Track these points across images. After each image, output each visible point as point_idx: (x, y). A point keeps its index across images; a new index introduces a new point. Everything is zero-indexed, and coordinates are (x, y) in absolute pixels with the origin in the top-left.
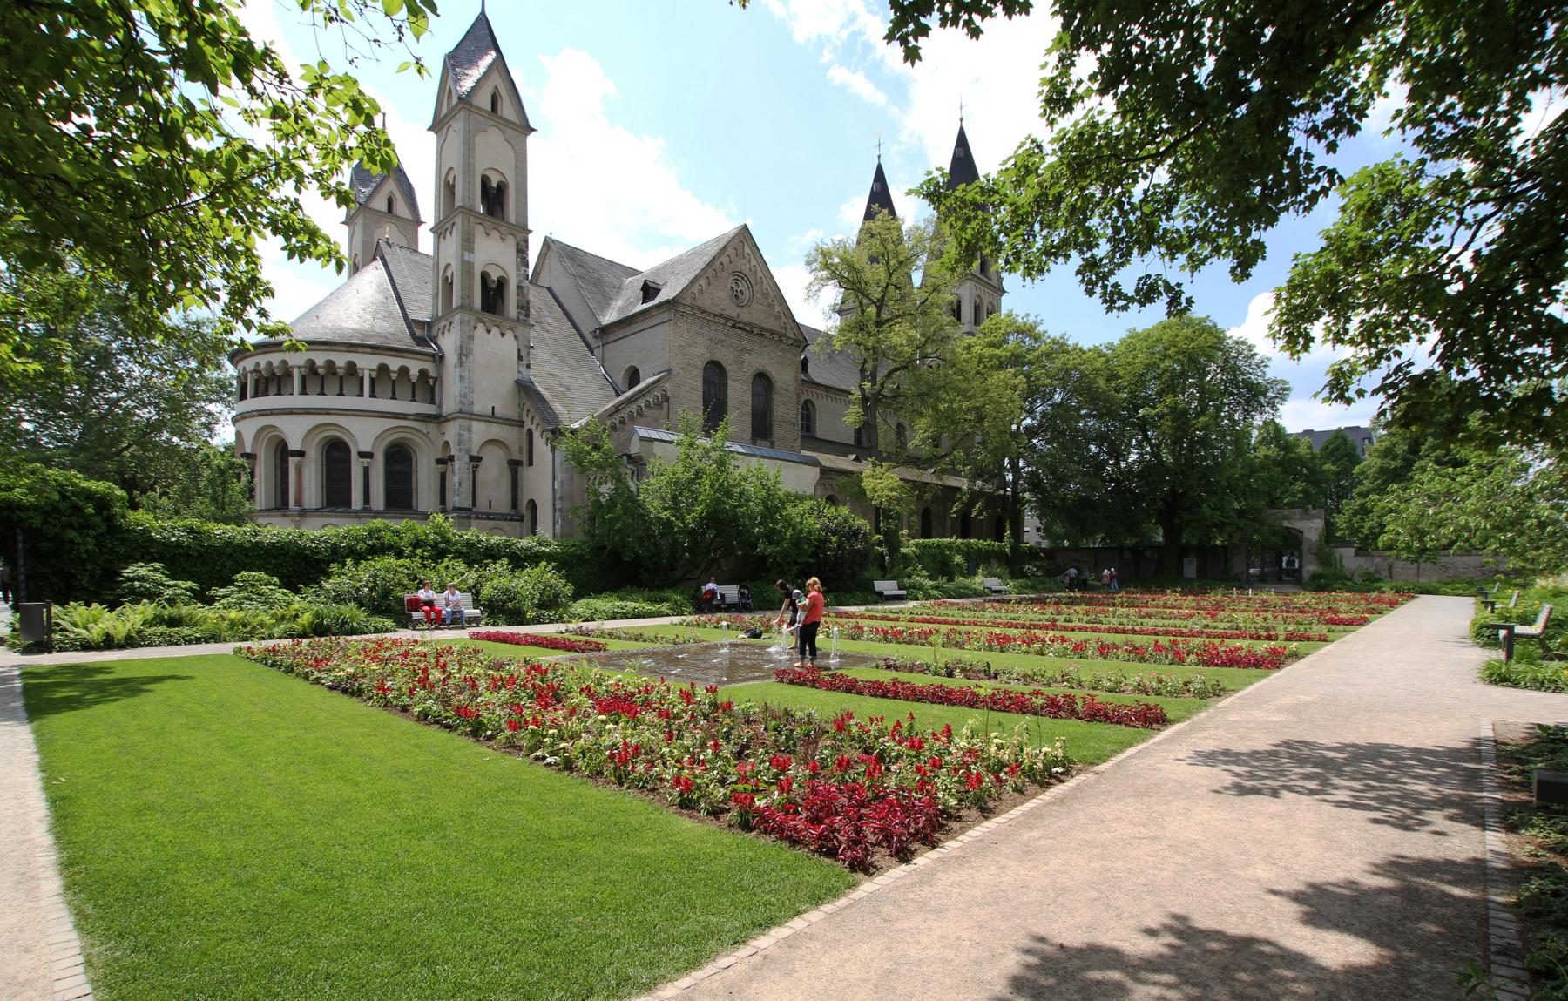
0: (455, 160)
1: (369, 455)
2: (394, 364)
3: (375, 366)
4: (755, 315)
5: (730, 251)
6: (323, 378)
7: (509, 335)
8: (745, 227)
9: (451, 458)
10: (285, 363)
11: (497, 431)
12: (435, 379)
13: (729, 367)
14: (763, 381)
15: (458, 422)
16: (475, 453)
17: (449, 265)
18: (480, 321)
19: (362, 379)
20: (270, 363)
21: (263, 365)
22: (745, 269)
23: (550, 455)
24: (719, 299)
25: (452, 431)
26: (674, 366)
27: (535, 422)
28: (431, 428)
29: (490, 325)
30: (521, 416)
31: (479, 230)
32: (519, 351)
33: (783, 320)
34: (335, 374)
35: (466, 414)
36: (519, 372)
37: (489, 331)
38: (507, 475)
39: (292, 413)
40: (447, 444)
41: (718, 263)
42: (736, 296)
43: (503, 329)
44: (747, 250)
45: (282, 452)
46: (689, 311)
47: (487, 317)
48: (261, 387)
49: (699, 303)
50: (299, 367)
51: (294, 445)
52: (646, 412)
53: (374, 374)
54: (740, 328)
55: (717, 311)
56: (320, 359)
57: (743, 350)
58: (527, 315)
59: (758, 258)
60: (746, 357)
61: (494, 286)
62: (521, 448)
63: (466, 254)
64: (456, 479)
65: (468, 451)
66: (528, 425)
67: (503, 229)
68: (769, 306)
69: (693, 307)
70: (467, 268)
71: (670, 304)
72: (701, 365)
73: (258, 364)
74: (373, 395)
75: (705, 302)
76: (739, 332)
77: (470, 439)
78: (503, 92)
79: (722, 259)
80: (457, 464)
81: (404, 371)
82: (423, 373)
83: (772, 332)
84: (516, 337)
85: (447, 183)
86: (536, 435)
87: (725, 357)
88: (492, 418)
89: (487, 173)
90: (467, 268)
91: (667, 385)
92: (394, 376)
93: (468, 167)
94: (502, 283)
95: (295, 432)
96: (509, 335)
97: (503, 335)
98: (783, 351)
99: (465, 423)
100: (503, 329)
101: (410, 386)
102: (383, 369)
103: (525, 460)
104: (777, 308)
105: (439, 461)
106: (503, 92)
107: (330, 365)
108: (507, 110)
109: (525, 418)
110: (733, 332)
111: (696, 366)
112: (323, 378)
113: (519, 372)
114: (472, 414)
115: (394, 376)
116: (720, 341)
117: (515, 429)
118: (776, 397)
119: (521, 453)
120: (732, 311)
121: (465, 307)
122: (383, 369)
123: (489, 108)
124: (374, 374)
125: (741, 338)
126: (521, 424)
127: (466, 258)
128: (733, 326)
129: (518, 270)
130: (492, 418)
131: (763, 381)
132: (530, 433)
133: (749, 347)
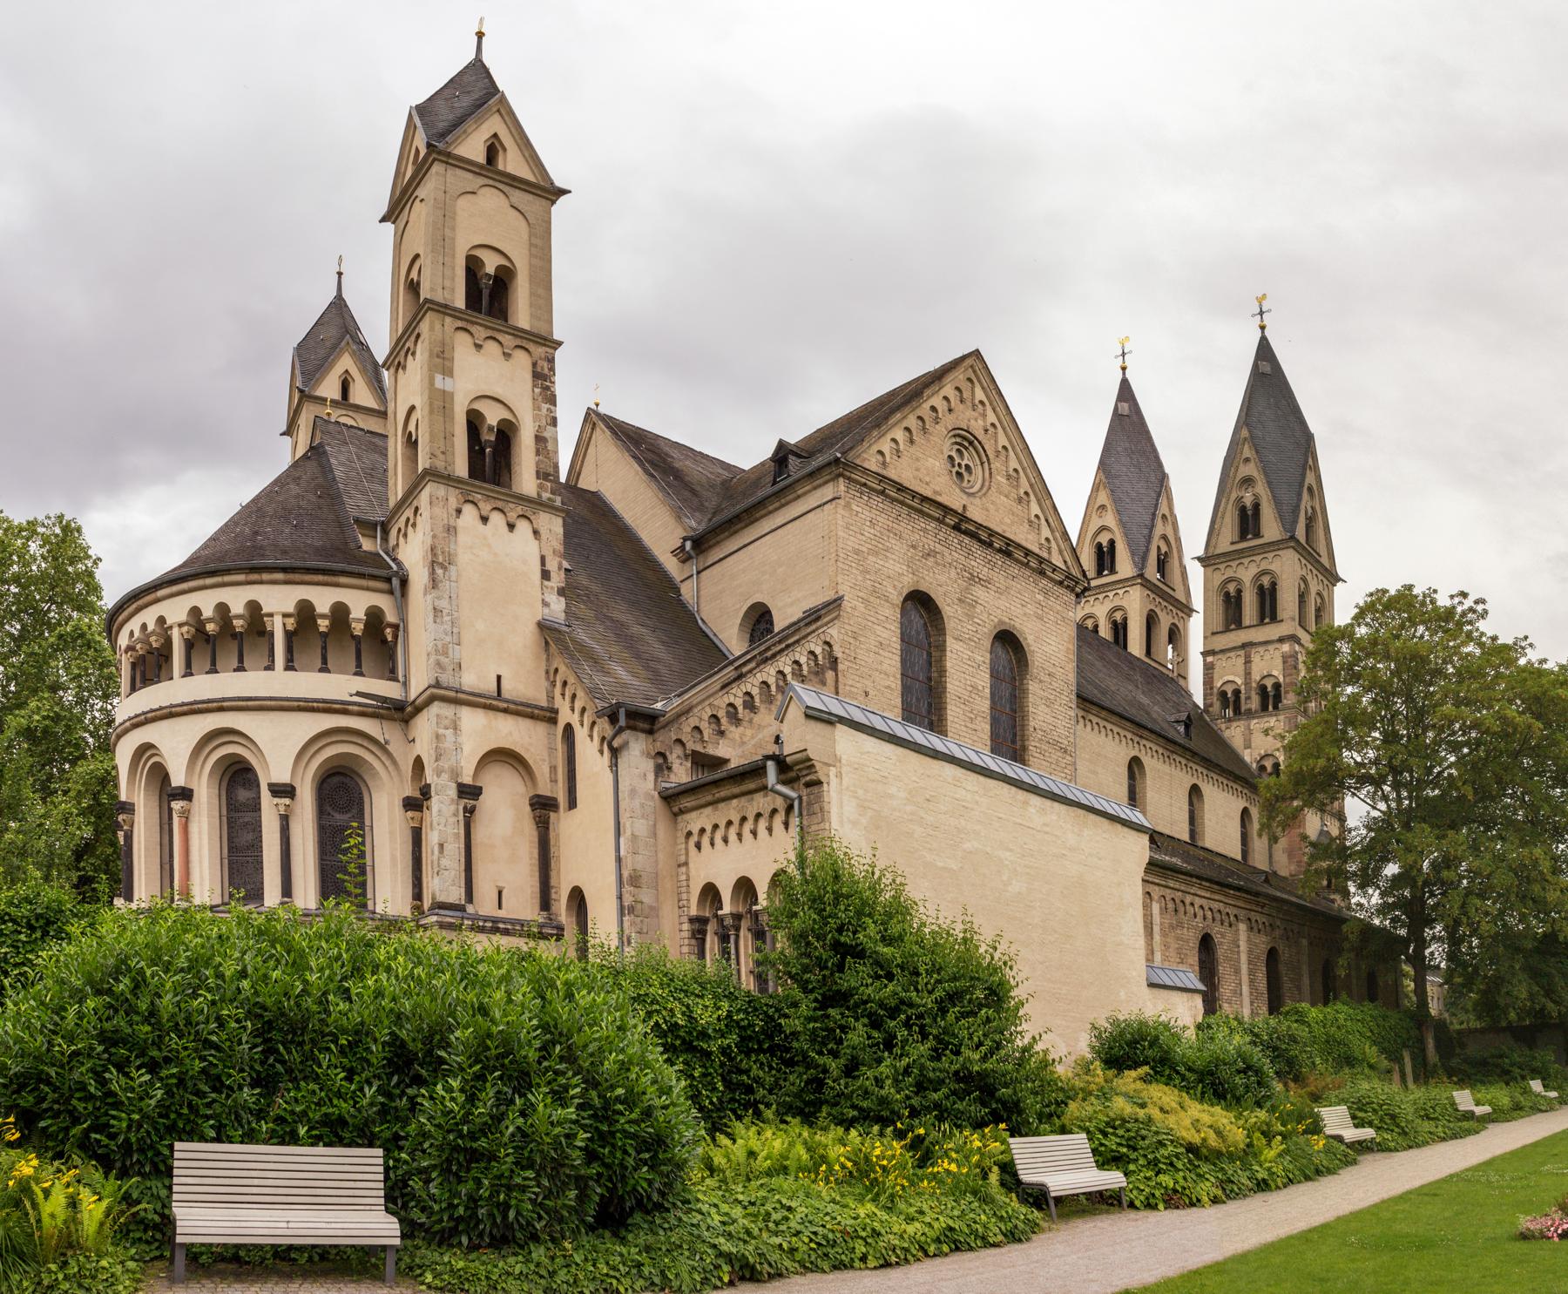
3: (291, 609)
7: (523, 527)
16: (467, 779)
17: (412, 408)
23: (608, 777)
27: (578, 705)
30: (551, 698)
35: (447, 695)
36: (545, 604)
37: (485, 520)
54: (967, 533)
62: (553, 769)
65: (455, 773)
66: (566, 716)
70: (441, 402)
77: (458, 748)
84: (536, 533)
86: (581, 734)
88: (495, 702)
90: (441, 402)
92: (323, 624)
97: (511, 527)
100: (512, 516)
102: (305, 612)
113: (545, 604)
124: (291, 622)
126: (550, 716)
128: (956, 528)
130: (495, 702)
132: (569, 729)
133: (984, 572)
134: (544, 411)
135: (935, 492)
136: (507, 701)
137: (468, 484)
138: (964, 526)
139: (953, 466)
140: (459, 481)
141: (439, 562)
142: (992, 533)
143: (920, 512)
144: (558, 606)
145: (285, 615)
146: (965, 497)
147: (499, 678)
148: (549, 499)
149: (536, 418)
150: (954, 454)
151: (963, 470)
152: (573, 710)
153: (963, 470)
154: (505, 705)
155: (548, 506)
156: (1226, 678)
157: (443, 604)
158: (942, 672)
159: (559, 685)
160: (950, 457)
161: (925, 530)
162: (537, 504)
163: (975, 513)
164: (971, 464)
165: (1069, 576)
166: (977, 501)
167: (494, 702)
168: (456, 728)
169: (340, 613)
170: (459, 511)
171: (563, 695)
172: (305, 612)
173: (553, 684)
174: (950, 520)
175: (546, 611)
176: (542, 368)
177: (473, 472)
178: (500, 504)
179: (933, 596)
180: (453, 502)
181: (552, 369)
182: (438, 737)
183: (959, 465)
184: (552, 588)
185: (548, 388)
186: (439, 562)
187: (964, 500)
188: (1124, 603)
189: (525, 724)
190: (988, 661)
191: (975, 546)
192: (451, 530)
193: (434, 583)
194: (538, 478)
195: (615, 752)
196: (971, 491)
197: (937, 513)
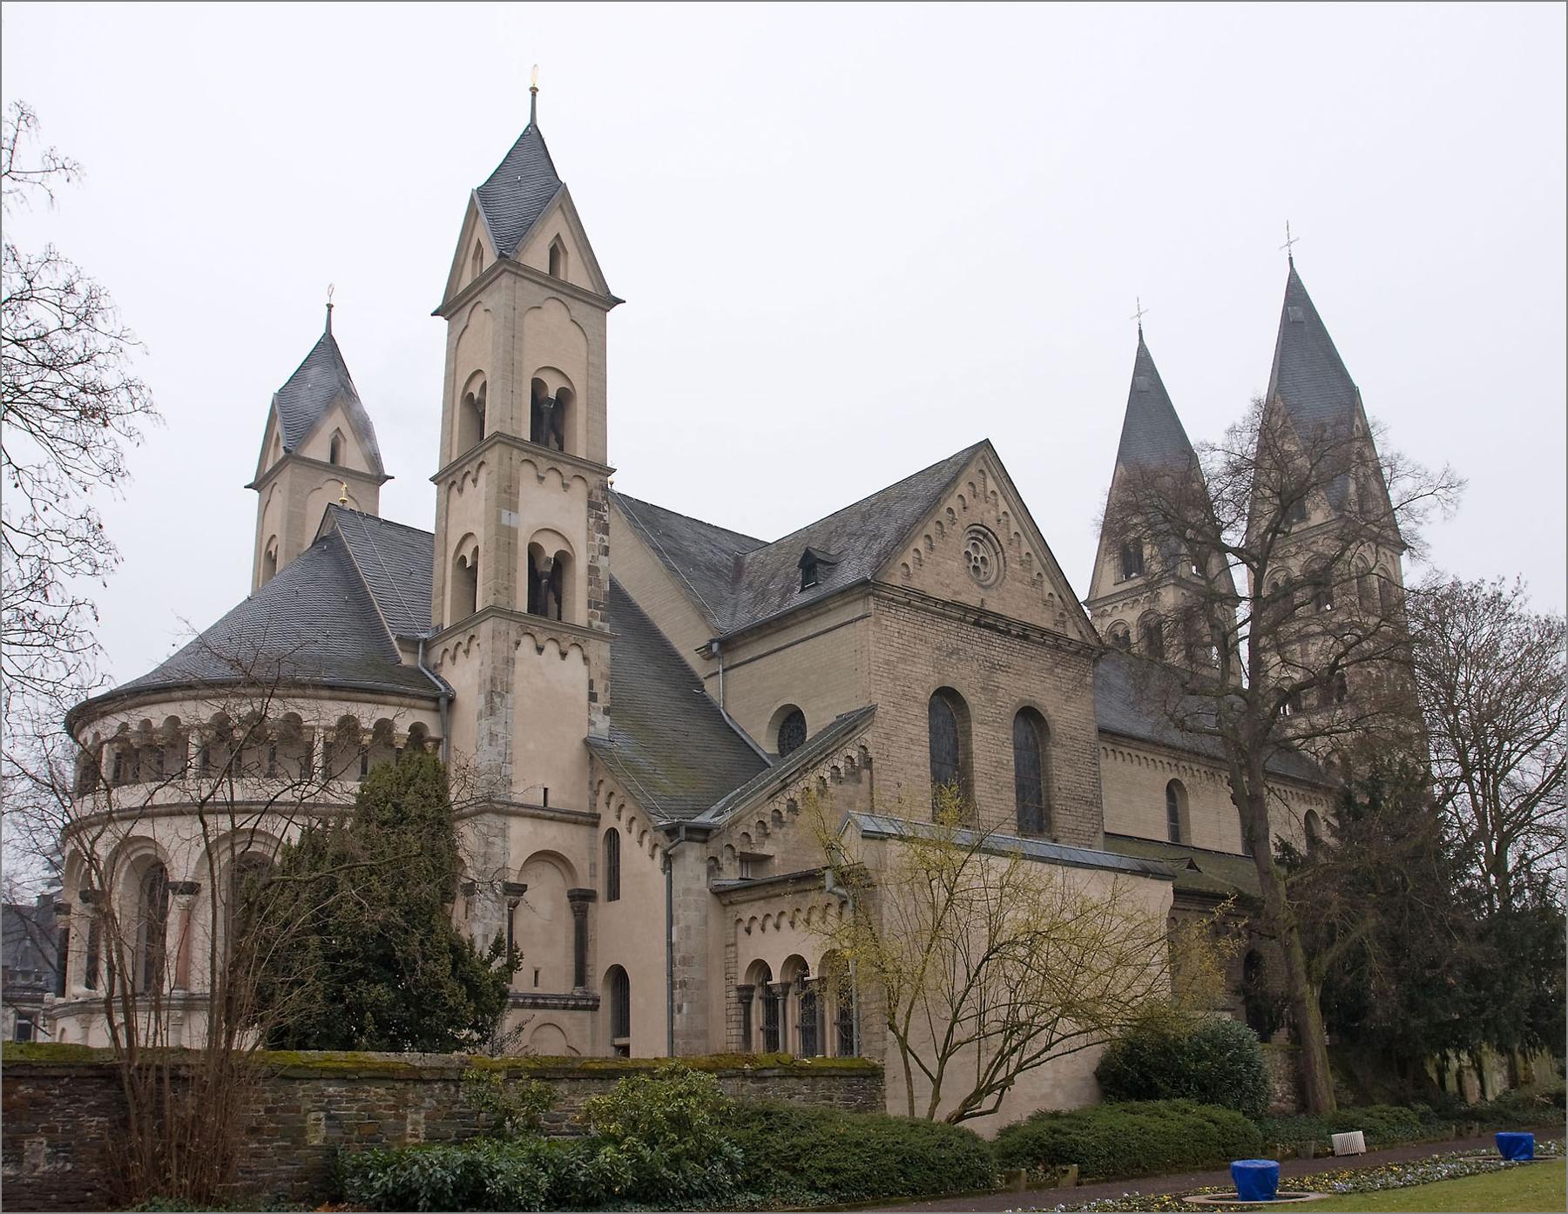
2: (368, 715)
4: (1013, 602)
7: (575, 655)
11: (553, 836)
13: (973, 699)
19: (310, 749)
26: (877, 699)
29: (542, 638)
32: (591, 683)
36: (591, 723)
37: (540, 650)
43: (565, 645)
49: (916, 584)
55: (946, 596)
57: (994, 667)
60: (1000, 678)
63: (505, 513)
68: (1034, 583)
69: (907, 591)
72: (924, 696)
76: (986, 632)
81: (384, 727)
84: (585, 659)
87: (965, 680)
88: (542, 813)
91: (868, 736)
92: (368, 738)
93: (512, 367)
96: (575, 655)
97: (564, 655)
100: (565, 645)
103: (601, 888)
109: (601, 808)
110: (975, 633)
113: (591, 723)
116: (955, 651)
117: (582, 832)
118: (1056, 753)
119: (593, 876)
120: (972, 598)
122: (348, 725)
125: (989, 644)
126: (593, 820)
127: (505, 521)
128: (976, 623)
130: (542, 813)
135: (956, 593)
137: (526, 618)
139: (970, 561)
140: (520, 615)
141: (496, 691)
143: (943, 615)
144: (603, 724)
146: (982, 591)
148: (599, 627)
149: (589, 548)
151: (979, 564)
153: (979, 564)
154: (552, 814)
155: (600, 635)
157: (499, 729)
159: (603, 795)
160: (967, 553)
162: (589, 632)
163: (993, 606)
164: (986, 556)
166: (994, 593)
167: (542, 813)
170: (518, 644)
171: (608, 804)
173: (597, 793)
175: (592, 729)
177: (533, 608)
178: (554, 635)
179: (947, 685)
180: (513, 636)
184: (599, 708)
186: (496, 691)
187: (983, 594)
192: (509, 662)
193: (492, 710)
194: (590, 607)
196: (988, 583)
197: (957, 614)
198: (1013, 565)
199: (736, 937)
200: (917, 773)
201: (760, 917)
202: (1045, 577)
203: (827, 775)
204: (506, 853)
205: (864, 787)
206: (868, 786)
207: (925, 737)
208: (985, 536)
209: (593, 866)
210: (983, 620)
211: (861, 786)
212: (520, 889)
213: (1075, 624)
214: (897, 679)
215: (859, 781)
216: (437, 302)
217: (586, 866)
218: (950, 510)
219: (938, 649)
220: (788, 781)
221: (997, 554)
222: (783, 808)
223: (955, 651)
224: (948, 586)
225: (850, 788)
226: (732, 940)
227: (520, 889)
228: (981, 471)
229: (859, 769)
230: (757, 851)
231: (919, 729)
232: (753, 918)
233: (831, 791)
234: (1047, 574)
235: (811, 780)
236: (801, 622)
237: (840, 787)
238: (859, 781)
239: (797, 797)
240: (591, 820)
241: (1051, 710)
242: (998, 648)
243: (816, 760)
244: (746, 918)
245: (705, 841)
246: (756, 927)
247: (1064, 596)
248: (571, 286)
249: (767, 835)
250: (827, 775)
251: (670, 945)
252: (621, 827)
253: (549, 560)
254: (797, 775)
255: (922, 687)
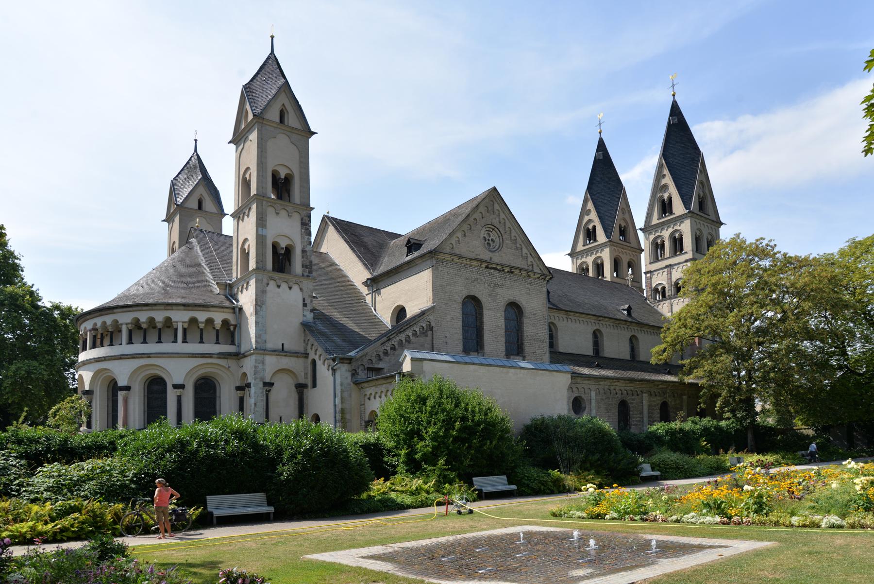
0: (251, 159)
1: (181, 387)
4: (507, 256)
5: (482, 209)
6: (145, 331)
8: (495, 189)
9: (248, 385)
10: (116, 321)
12: (235, 326)
13: (484, 300)
14: (514, 310)
15: (253, 357)
18: (271, 278)
19: (176, 330)
20: (104, 323)
21: (99, 325)
22: (496, 222)
23: (332, 378)
24: (474, 246)
25: (248, 365)
27: (318, 353)
28: (232, 363)
29: (279, 282)
30: (306, 349)
31: (270, 211)
33: (530, 259)
34: (155, 327)
38: (295, 396)
39: (121, 358)
40: (245, 374)
41: (472, 219)
42: (488, 243)
43: (291, 284)
44: (497, 207)
45: (114, 388)
46: (448, 258)
47: (277, 275)
48: (98, 342)
49: (457, 251)
50: (127, 324)
51: (122, 383)
52: (413, 339)
53: (186, 326)
55: (473, 256)
56: (143, 317)
57: (496, 286)
58: (311, 272)
59: (507, 212)
60: (499, 290)
61: (283, 252)
63: (260, 229)
64: (252, 401)
66: (312, 356)
67: (290, 209)
68: (517, 249)
69: (451, 254)
71: (432, 253)
72: (460, 299)
73: (95, 324)
74: (185, 341)
75: (462, 250)
76: (492, 271)
78: (289, 108)
79: (475, 216)
80: (253, 389)
81: (210, 321)
82: (225, 323)
83: (521, 270)
85: (244, 179)
86: (319, 364)
87: (480, 292)
88: (282, 351)
89: (278, 169)
94: (289, 250)
95: (123, 373)
96: (296, 288)
98: (531, 284)
99: (260, 357)
101: (214, 333)
102: (193, 321)
104: (525, 250)
105: (238, 388)
106: (289, 108)
107: (152, 320)
108: (292, 120)
109: (309, 351)
110: (486, 271)
111: (455, 301)
112: (145, 331)
114: (265, 350)
115: (202, 326)
116: (476, 280)
117: (301, 361)
118: (526, 321)
119: (306, 378)
120: (486, 255)
121: (260, 267)
123: (278, 120)
124: (186, 326)
127: (260, 232)
128: (487, 267)
129: (302, 238)
130: (282, 351)
131: (514, 310)
132: (314, 362)
133: (501, 282)
134: (306, 239)
135: (477, 255)
136: (286, 352)
138: (490, 266)
139: (486, 241)
142: (503, 266)
145: (183, 322)
146: (491, 253)
147: (283, 344)
150: (485, 236)
151: (490, 242)
152: (316, 354)
153: (490, 242)
154: (285, 354)
156: (657, 283)
158: (482, 323)
159: (309, 346)
160: (484, 237)
161: (472, 272)
164: (494, 238)
165: (542, 275)
166: (497, 254)
167: (281, 353)
168: (263, 363)
169: (210, 321)
171: (312, 349)
172: (193, 321)
173: (307, 344)
174: (484, 265)
176: (305, 220)
181: (310, 221)
182: (255, 367)
183: (489, 240)
185: (308, 229)
187: (491, 254)
188: (601, 255)
189: (293, 359)
190: (503, 315)
191: (496, 273)
195: (334, 371)
196: (494, 249)
198: (507, 242)
199: (364, 401)
200: (455, 332)
201: (373, 394)
202: (523, 246)
203: (410, 334)
204: (264, 370)
205: (429, 338)
206: (431, 338)
207: (460, 316)
208: (493, 229)
209: (306, 374)
210: (489, 265)
211: (427, 338)
212: (272, 384)
213: (538, 266)
214: (446, 292)
215: (427, 336)
216: (230, 138)
217: (303, 374)
218: (475, 219)
219: (467, 279)
220: (391, 337)
221: (499, 237)
222: (388, 349)
223: (476, 280)
224: (473, 252)
225: (422, 339)
226: (363, 403)
227: (272, 384)
228: (492, 201)
229: (427, 331)
230: (376, 366)
231: (456, 313)
232: (371, 394)
233: (412, 340)
234: (524, 245)
235: (402, 337)
236: (405, 270)
237: (417, 339)
238: (427, 336)
239: (396, 344)
240: (304, 355)
241: (524, 304)
242: (498, 278)
243: (404, 328)
244: (368, 394)
245: (350, 363)
246: (372, 397)
247: (532, 254)
248: (293, 128)
249: (380, 360)
250: (410, 334)
251: (335, 405)
252: (317, 358)
253: (283, 248)
254: (395, 335)
255: (459, 296)
